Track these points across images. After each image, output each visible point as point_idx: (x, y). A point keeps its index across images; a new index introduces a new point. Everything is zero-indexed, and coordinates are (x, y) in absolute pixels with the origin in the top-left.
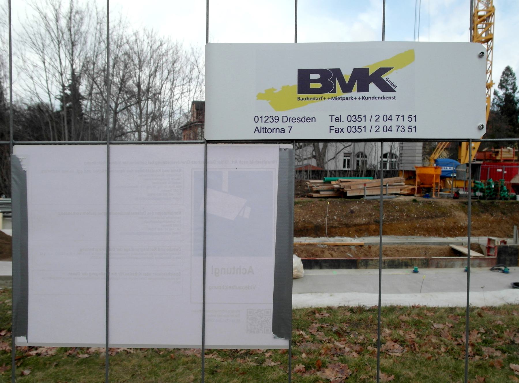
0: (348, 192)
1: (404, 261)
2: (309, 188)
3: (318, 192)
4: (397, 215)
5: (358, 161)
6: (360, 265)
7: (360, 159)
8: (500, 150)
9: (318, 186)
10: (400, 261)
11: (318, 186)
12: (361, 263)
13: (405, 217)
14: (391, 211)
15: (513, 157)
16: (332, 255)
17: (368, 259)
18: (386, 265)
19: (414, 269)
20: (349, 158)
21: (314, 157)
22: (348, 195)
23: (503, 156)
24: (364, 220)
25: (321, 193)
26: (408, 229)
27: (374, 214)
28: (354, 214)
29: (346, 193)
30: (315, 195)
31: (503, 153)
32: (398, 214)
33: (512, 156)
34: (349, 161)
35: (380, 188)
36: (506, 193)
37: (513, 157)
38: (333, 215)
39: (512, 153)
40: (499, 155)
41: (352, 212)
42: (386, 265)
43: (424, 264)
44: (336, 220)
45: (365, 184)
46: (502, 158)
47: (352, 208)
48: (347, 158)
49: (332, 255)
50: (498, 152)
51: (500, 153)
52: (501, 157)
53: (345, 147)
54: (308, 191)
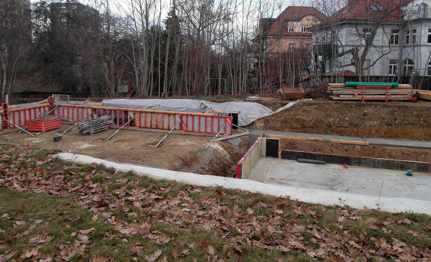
1: (400, 163)
2: (329, 92)
3: (338, 95)
4: (412, 119)
5: (405, 67)
6: (353, 162)
7: (407, 65)
9: (339, 90)
10: (396, 163)
11: (339, 90)
12: (354, 160)
13: (421, 123)
14: (407, 115)
16: (332, 151)
17: (362, 158)
18: (380, 165)
19: (407, 172)
20: (395, 64)
21: (353, 64)
24: (376, 122)
25: (341, 96)
26: (423, 134)
27: (387, 117)
28: (366, 117)
30: (335, 98)
32: (414, 119)
34: (395, 66)
38: (345, 117)
41: (365, 114)
42: (380, 165)
43: (422, 168)
44: (347, 121)
47: (366, 111)
49: (332, 151)
53: (384, 55)
54: (329, 94)
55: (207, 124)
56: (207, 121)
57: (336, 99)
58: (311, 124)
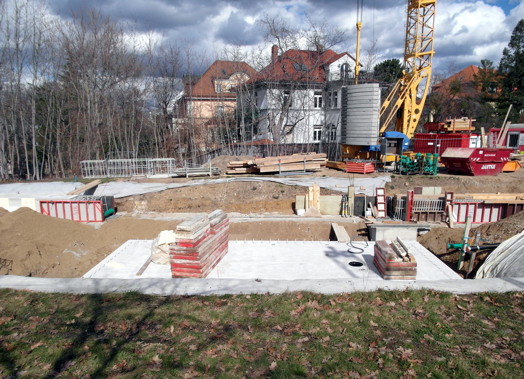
0: (261, 168)
8: (452, 120)
15: (469, 128)
22: (261, 171)
23: (455, 127)
29: (259, 169)
31: (455, 123)
33: (468, 126)
34: (320, 132)
35: (303, 163)
36: (431, 168)
37: (469, 128)
39: (469, 123)
40: (452, 126)
45: (279, 161)
46: (455, 129)
48: (317, 130)
50: (450, 123)
51: (452, 123)
52: (453, 128)
55: (73, 212)
56: (73, 208)
57: (232, 173)
58: (198, 203)
